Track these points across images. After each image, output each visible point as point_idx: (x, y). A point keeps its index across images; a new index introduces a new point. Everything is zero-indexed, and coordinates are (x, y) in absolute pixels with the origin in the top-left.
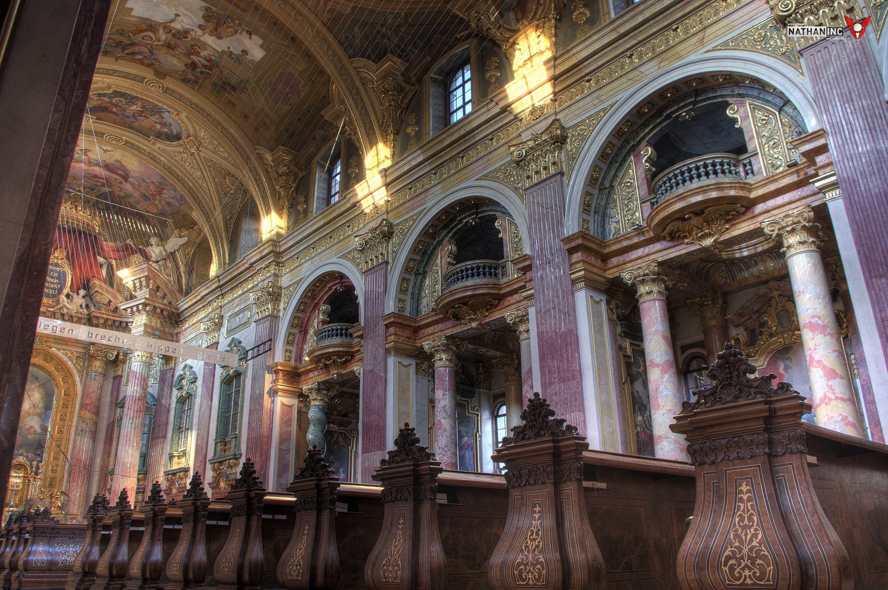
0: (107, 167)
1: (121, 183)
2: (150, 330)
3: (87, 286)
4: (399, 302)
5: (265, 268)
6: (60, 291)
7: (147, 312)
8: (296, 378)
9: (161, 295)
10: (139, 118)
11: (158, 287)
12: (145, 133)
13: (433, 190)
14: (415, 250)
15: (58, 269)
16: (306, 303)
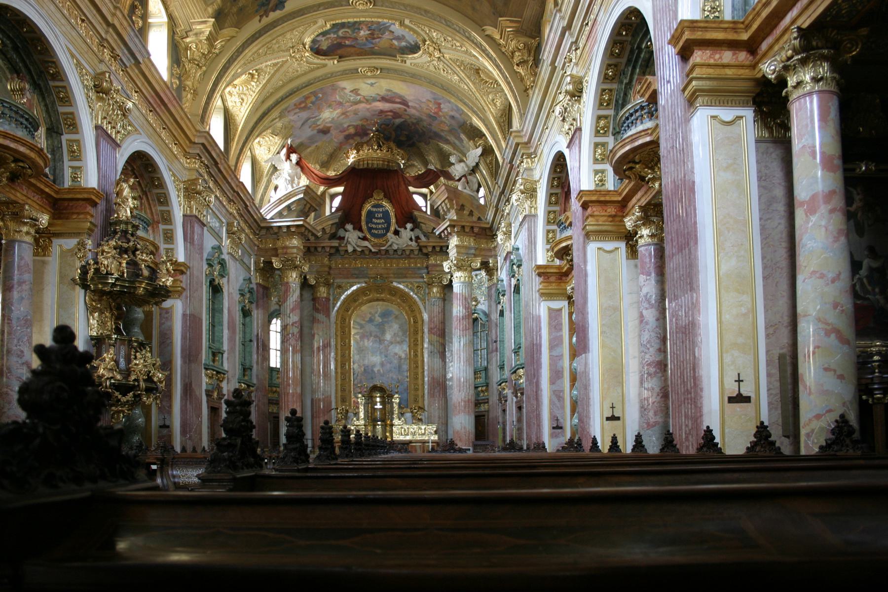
0: (384, 99)
1: (405, 110)
2: (463, 251)
3: (411, 219)
4: (596, 174)
5: (520, 164)
6: (387, 230)
7: (459, 234)
8: (564, 278)
9: (468, 213)
10: (374, 41)
11: (463, 206)
12: (390, 53)
13: (599, 19)
14: (601, 104)
15: (381, 210)
16: (556, 194)
